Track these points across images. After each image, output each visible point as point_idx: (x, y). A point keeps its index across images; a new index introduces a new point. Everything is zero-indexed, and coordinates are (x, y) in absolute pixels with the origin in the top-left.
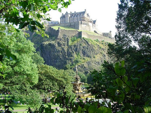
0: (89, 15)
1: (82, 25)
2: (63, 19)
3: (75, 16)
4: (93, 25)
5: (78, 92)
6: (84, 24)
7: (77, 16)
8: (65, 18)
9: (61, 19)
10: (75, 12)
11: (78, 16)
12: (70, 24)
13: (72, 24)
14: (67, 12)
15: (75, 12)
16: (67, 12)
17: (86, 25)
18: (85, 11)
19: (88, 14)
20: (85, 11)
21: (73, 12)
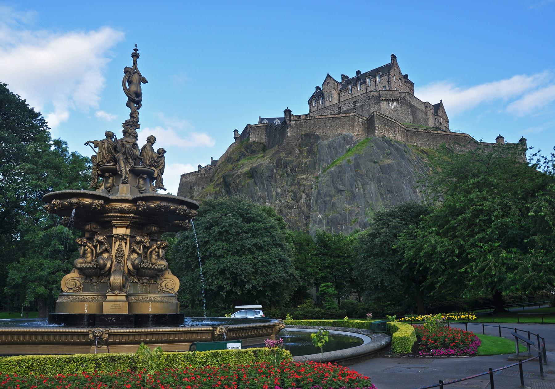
0: (410, 78)
1: (384, 105)
2: (317, 101)
3: (358, 84)
4: (426, 107)
5: (101, 307)
6: (388, 100)
7: (365, 82)
8: (323, 98)
9: (310, 102)
10: (358, 72)
11: (368, 80)
12: (339, 108)
13: (345, 108)
14: (329, 76)
15: (358, 72)
16: (329, 76)
17: (396, 104)
18: (389, 61)
19: (406, 76)
20: (389, 61)
21: (352, 75)
